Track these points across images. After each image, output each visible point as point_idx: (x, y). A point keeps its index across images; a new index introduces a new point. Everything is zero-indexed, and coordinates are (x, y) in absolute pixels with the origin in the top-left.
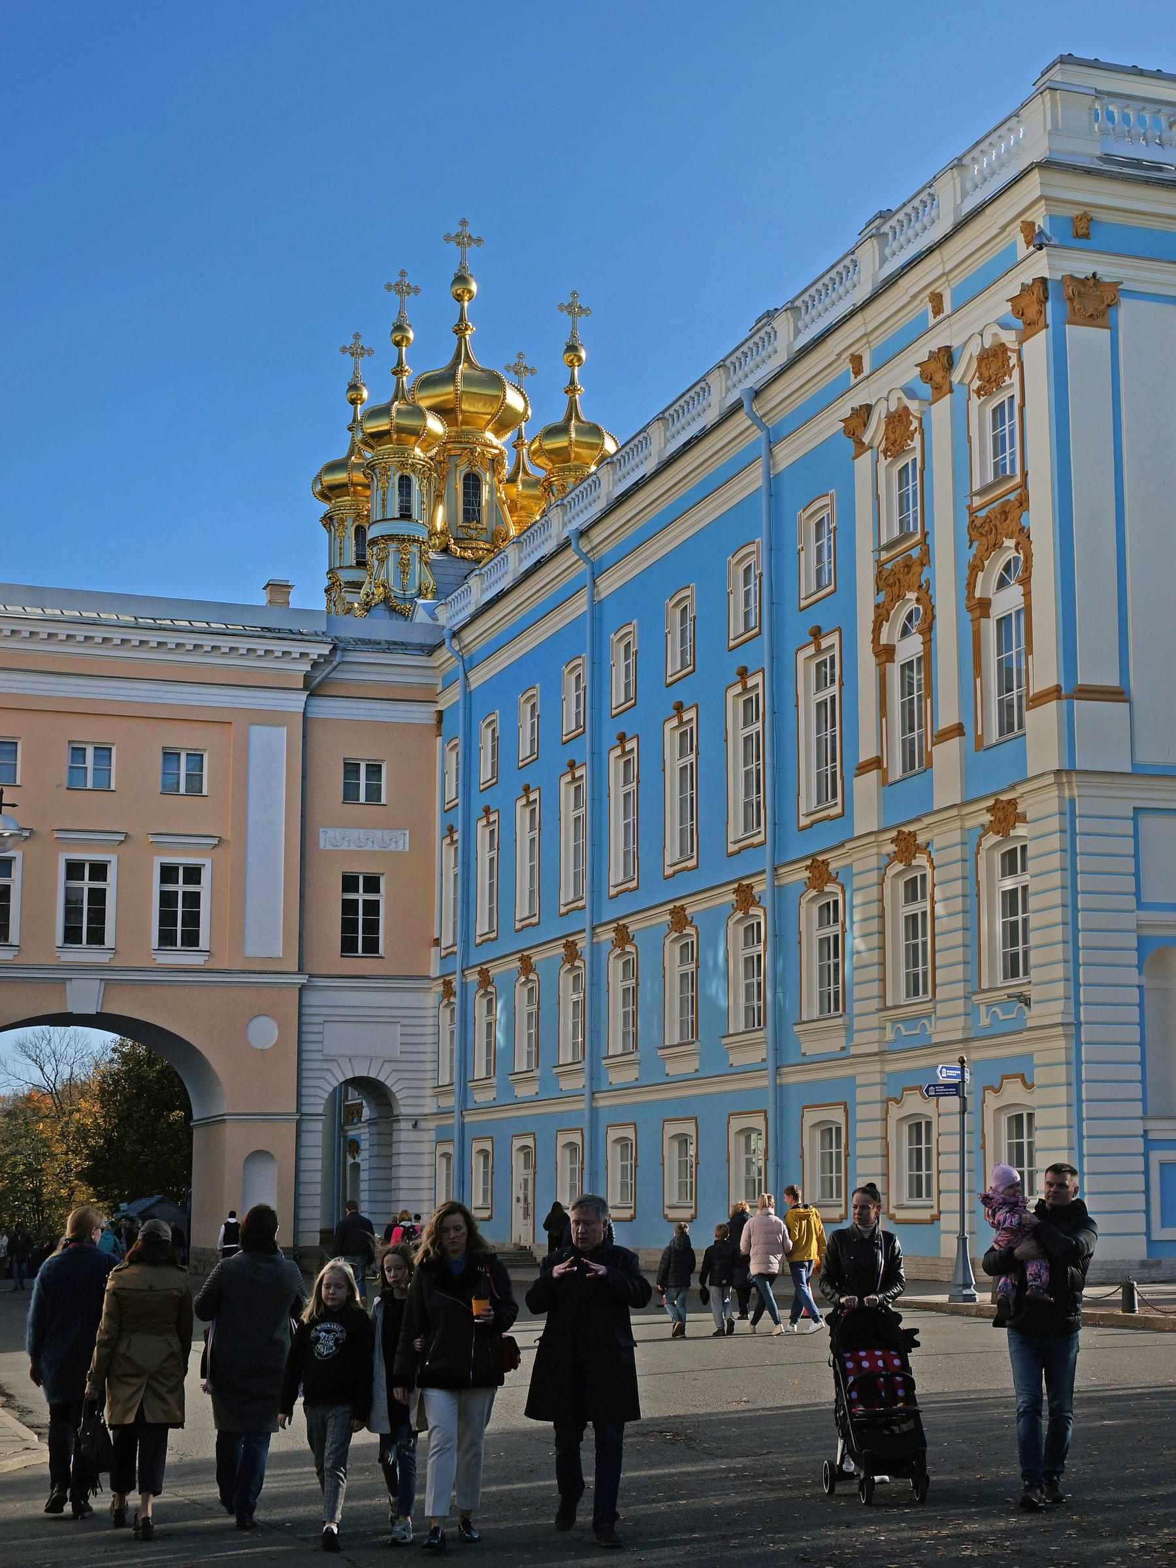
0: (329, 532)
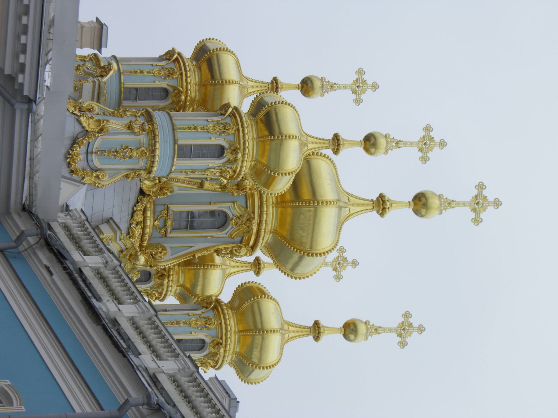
0: (161, 58)
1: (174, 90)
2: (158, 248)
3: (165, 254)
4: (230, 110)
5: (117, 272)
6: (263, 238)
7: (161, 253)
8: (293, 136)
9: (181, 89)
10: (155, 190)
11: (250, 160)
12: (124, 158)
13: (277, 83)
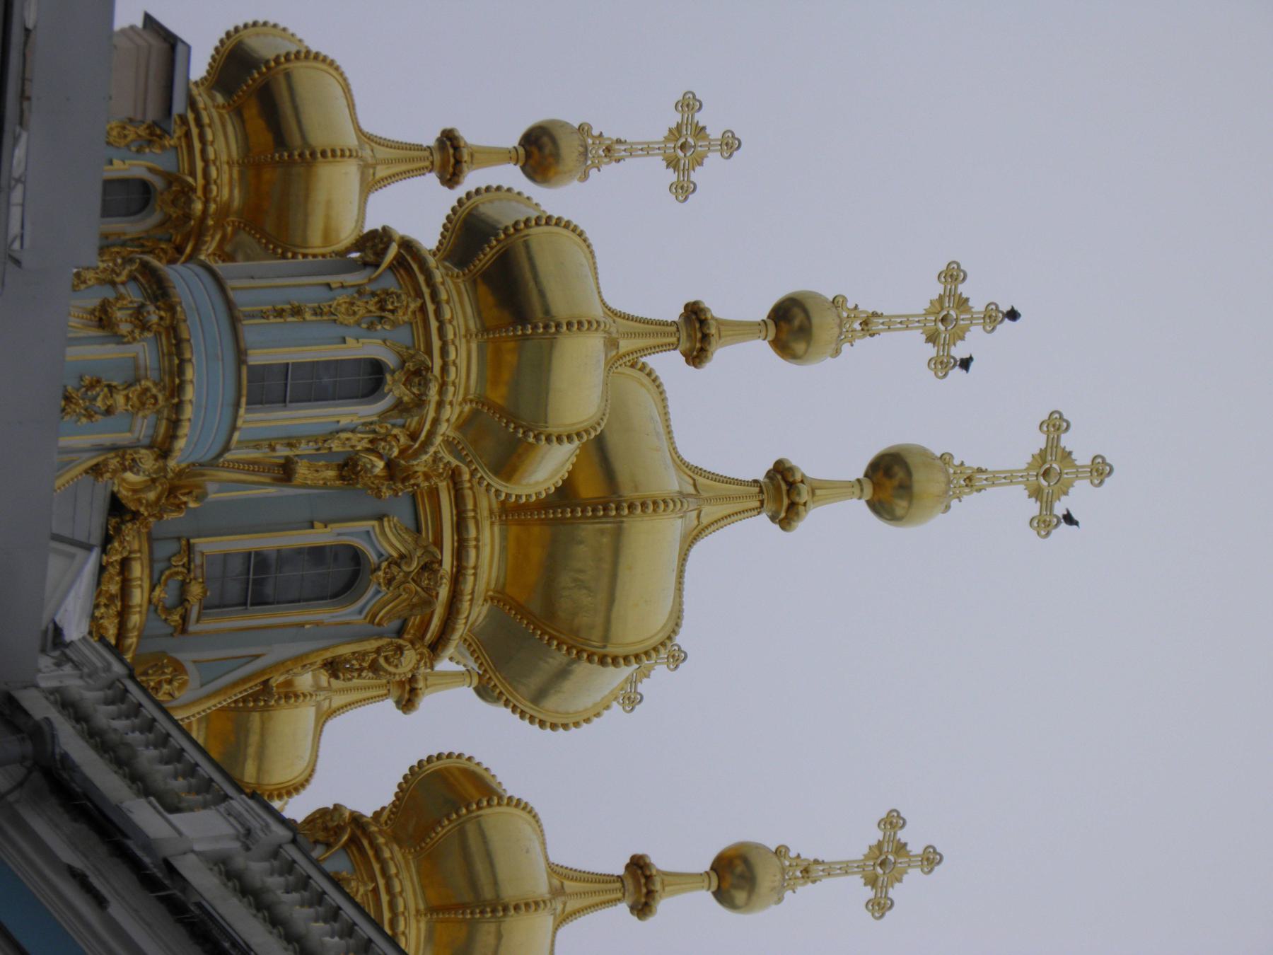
1: (170, 184)
2: (163, 667)
3: (183, 684)
4: (393, 250)
5: (290, 867)
6: (467, 618)
7: (170, 682)
8: (590, 323)
9: (190, 180)
10: (152, 496)
11: (460, 398)
12: (90, 417)
13: (456, 148)
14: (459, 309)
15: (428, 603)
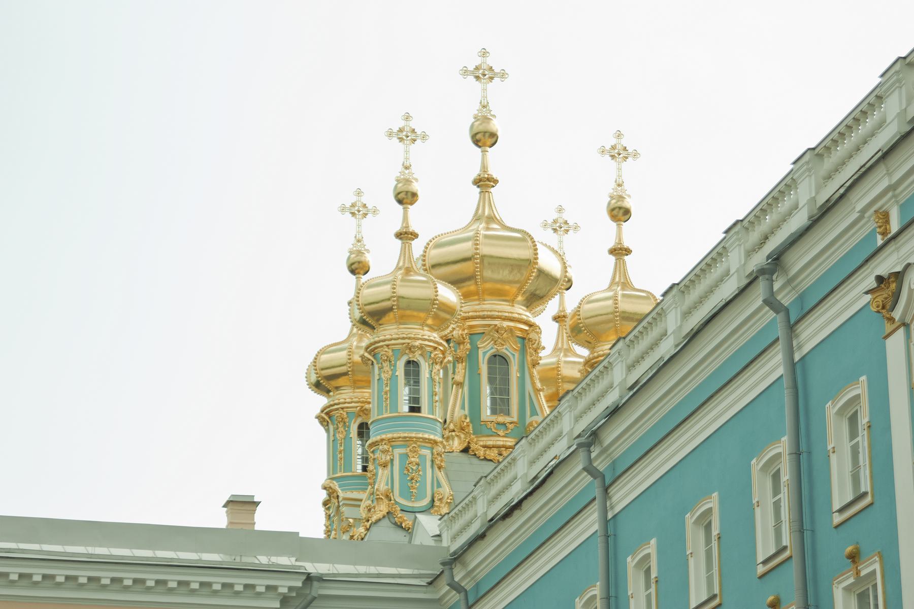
0: (327, 431)
4: (366, 355)
10: (463, 436)
14: (389, 331)
15: (511, 330)
